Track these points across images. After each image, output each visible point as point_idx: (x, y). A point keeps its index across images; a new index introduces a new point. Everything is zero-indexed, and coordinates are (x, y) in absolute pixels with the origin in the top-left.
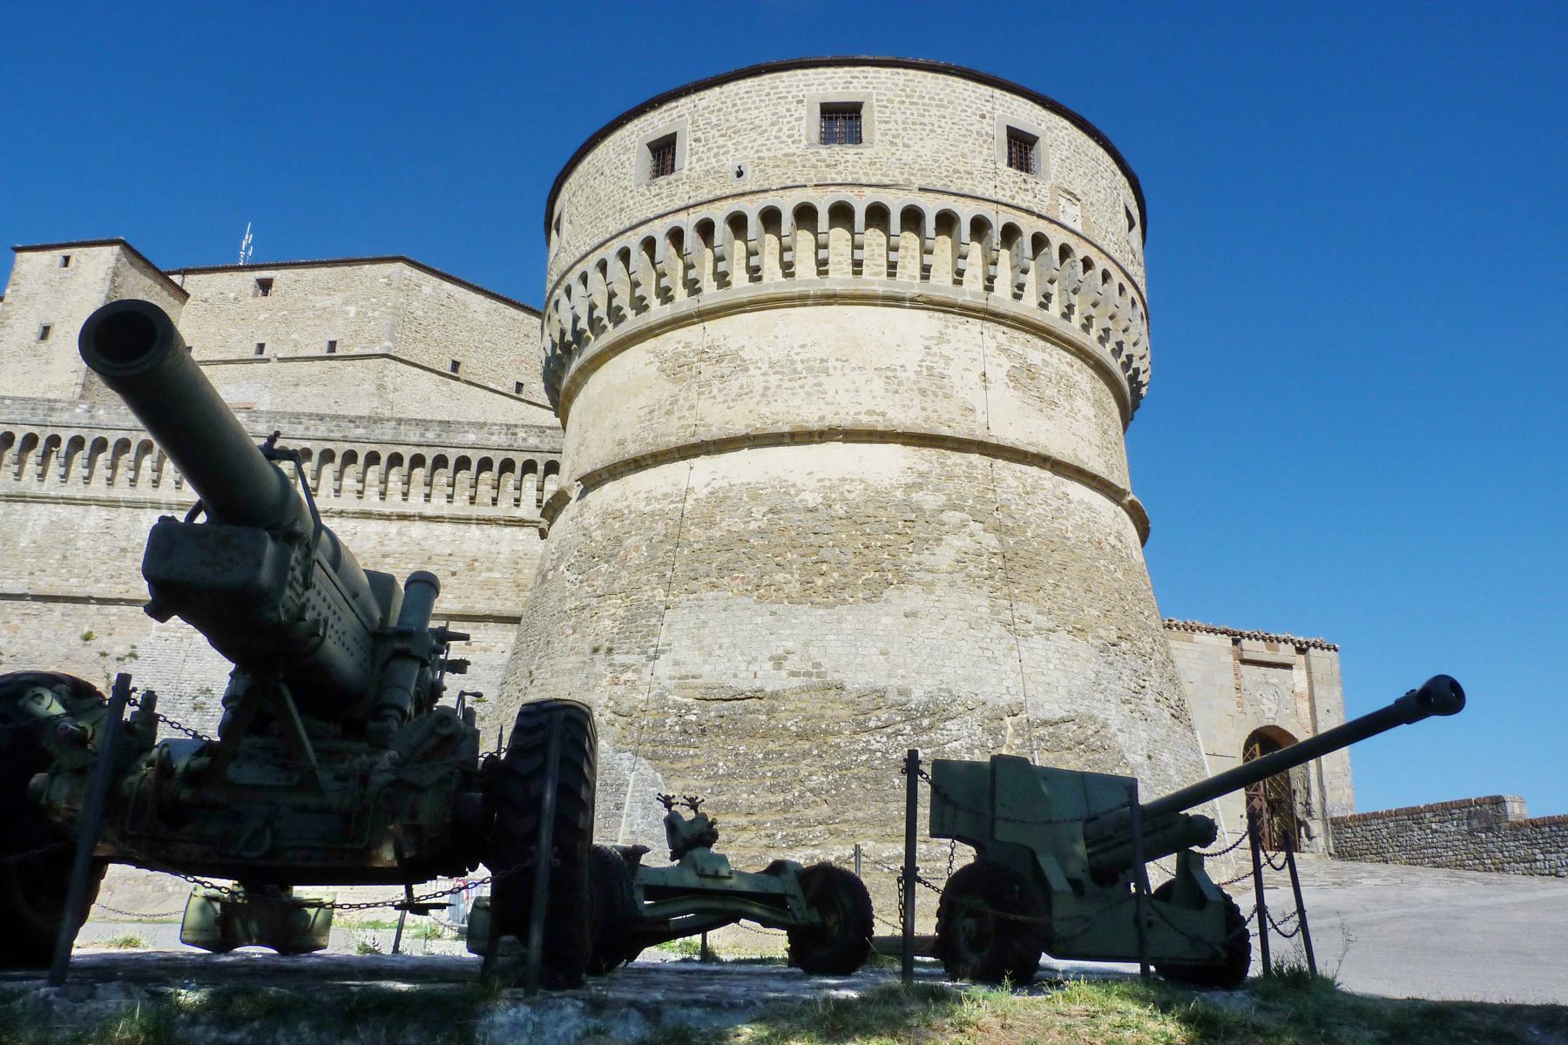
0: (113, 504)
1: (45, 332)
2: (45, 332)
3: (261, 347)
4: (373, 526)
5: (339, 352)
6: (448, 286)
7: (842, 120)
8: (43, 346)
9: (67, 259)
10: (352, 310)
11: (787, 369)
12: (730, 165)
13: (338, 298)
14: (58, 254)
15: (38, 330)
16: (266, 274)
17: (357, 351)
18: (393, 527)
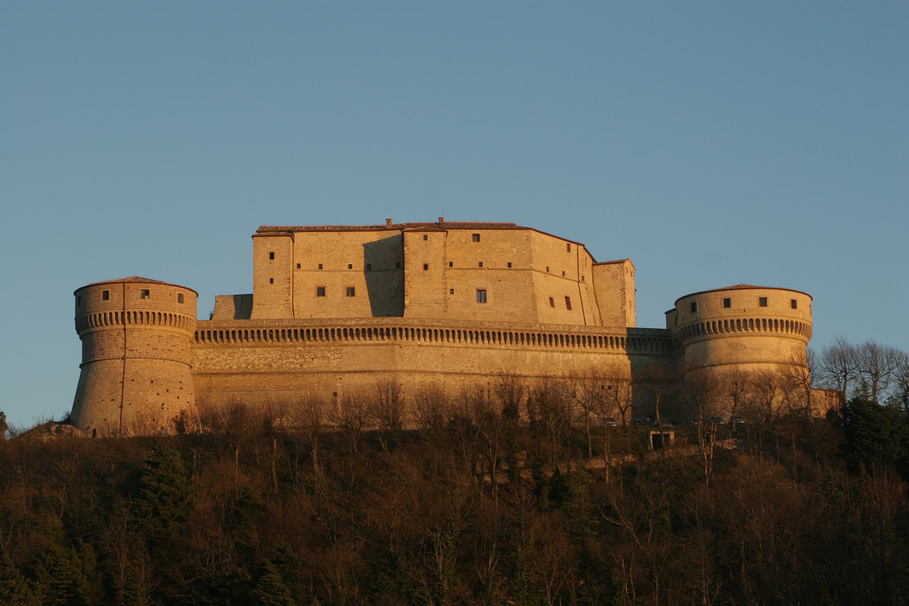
0: (547, 351)
1: (426, 267)
2: (426, 267)
3: (481, 264)
4: (610, 356)
5: (513, 267)
6: (543, 236)
7: (763, 302)
8: (426, 272)
9: (426, 238)
10: (515, 250)
11: (753, 349)
12: (742, 308)
13: (508, 244)
14: (422, 234)
15: (421, 267)
16: (477, 232)
17: (520, 267)
18: (615, 357)
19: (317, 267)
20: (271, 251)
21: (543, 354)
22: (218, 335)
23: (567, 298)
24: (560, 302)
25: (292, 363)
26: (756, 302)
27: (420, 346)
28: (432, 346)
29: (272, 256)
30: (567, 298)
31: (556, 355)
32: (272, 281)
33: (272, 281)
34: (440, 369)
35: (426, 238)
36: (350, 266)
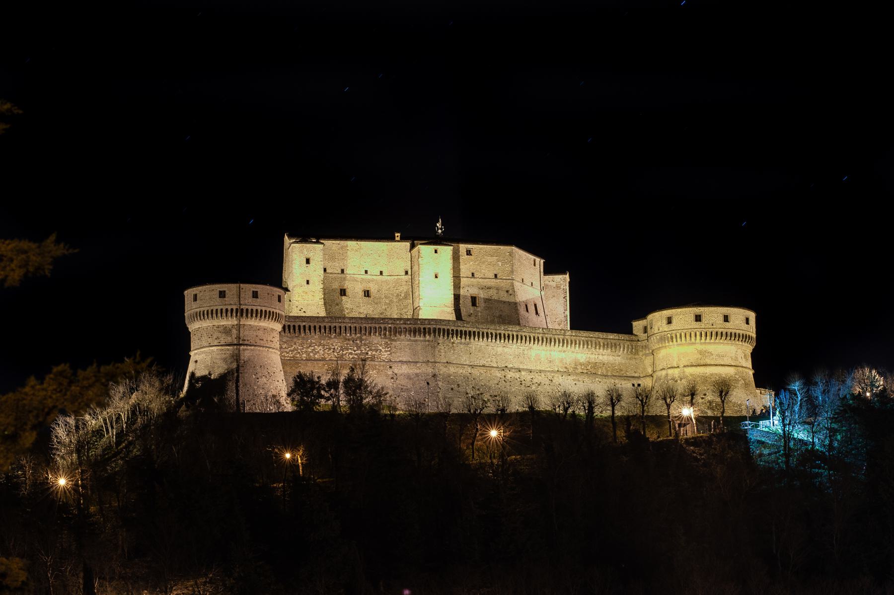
3: (473, 274)
7: (726, 319)
9: (436, 252)
11: (718, 355)
19: (340, 271)
20: (308, 257)
21: (543, 353)
22: (292, 328)
23: (535, 305)
24: (532, 309)
25: (351, 354)
26: (722, 318)
27: (453, 343)
28: (461, 343)
29: (308, 261)
30: (535, 305)
31: (552, 353)
32: (308, 282)
33: (308, 282)
34: (467, 363)
35: (436, 252)
36: (366, 272)
